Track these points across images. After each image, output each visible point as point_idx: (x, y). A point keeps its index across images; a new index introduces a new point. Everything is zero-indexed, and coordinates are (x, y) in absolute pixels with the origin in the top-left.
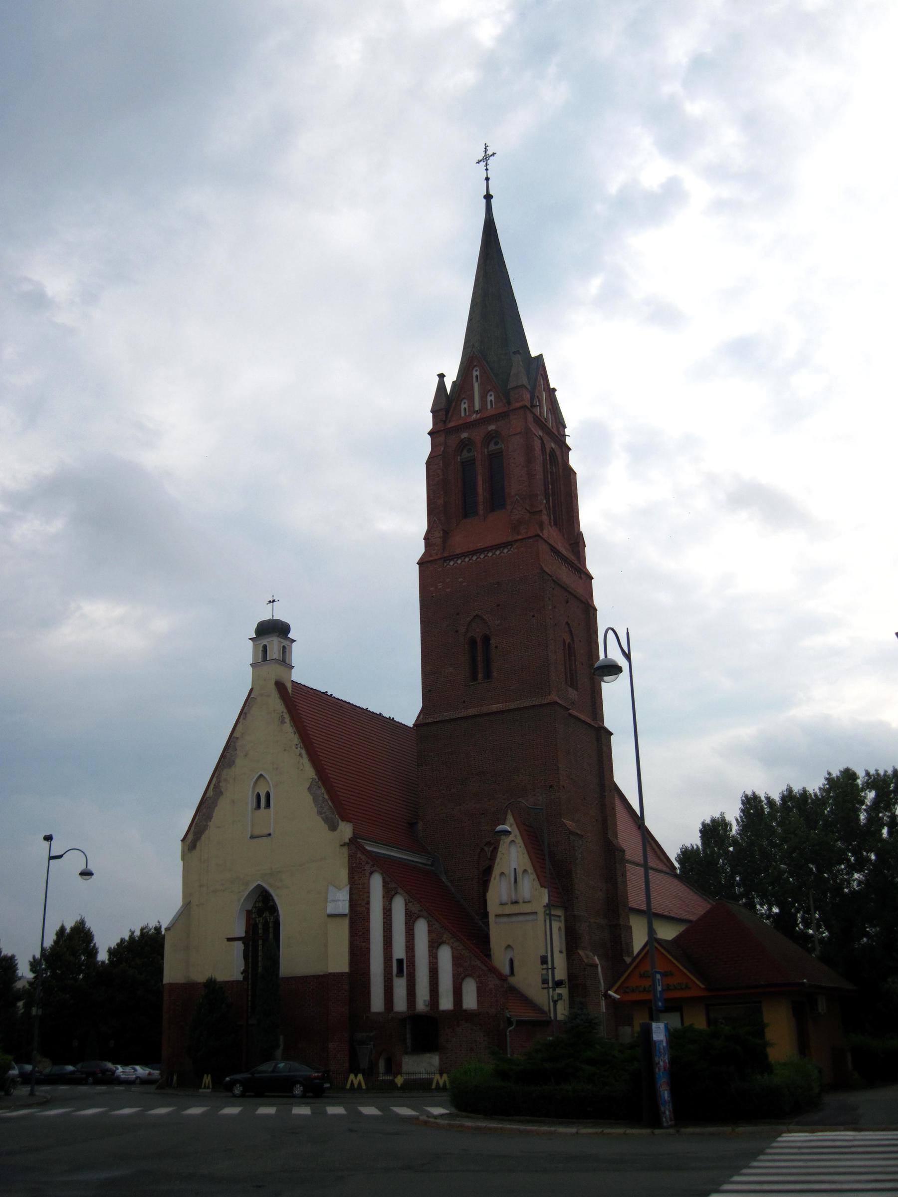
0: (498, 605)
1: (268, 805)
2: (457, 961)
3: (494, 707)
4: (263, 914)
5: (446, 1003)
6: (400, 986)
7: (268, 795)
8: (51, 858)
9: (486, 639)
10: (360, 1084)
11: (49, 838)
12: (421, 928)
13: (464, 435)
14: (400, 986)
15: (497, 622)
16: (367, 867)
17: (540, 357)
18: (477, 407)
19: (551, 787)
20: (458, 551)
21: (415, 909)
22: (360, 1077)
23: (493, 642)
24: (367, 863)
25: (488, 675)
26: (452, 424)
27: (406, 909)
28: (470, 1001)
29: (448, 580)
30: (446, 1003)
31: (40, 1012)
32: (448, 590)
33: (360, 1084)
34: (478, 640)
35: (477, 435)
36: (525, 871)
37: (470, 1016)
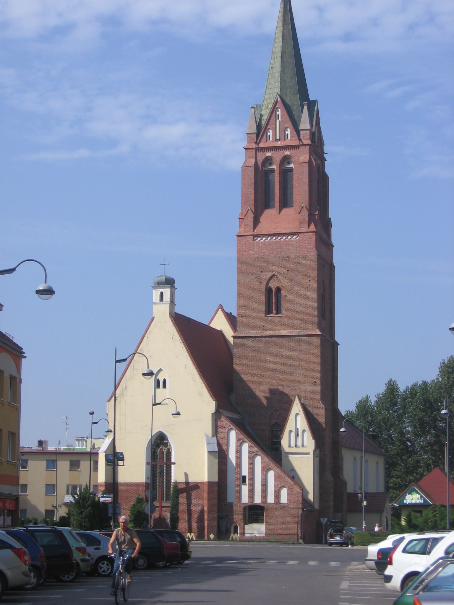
0: (288, 271)
1: (165, 386)
2: (277, 478)
3: (284, 332)
4: (159, 446)
5: (271, 499)
6: (245, 489)
7: (165, 381)
8: (93, 423)
9: (278, 290)
10: (192, 538)
11: (92, 414)
12: (258, 460)
13: (268, 154)
14: (245, 489)
15: (287, 281)
16: (226, 426)
17: (315, 101)
18: (278, 138)
19: (315, 382)
20: (264, 232)
21: (255, 449)
22: (192, 534)
23: (283, 292)
24: (227, 424)
25: (278, 311)
26: (261, 145)
27: (249, 450)
28: (284, 499)
29: (256, 250)
30: (271, 499)
31: (322, 519)
32: (256, 256)
33: (192, 538)
34: (274, 290)
35: (277, 156)
36: (304, 431)
37: (284, 506)
